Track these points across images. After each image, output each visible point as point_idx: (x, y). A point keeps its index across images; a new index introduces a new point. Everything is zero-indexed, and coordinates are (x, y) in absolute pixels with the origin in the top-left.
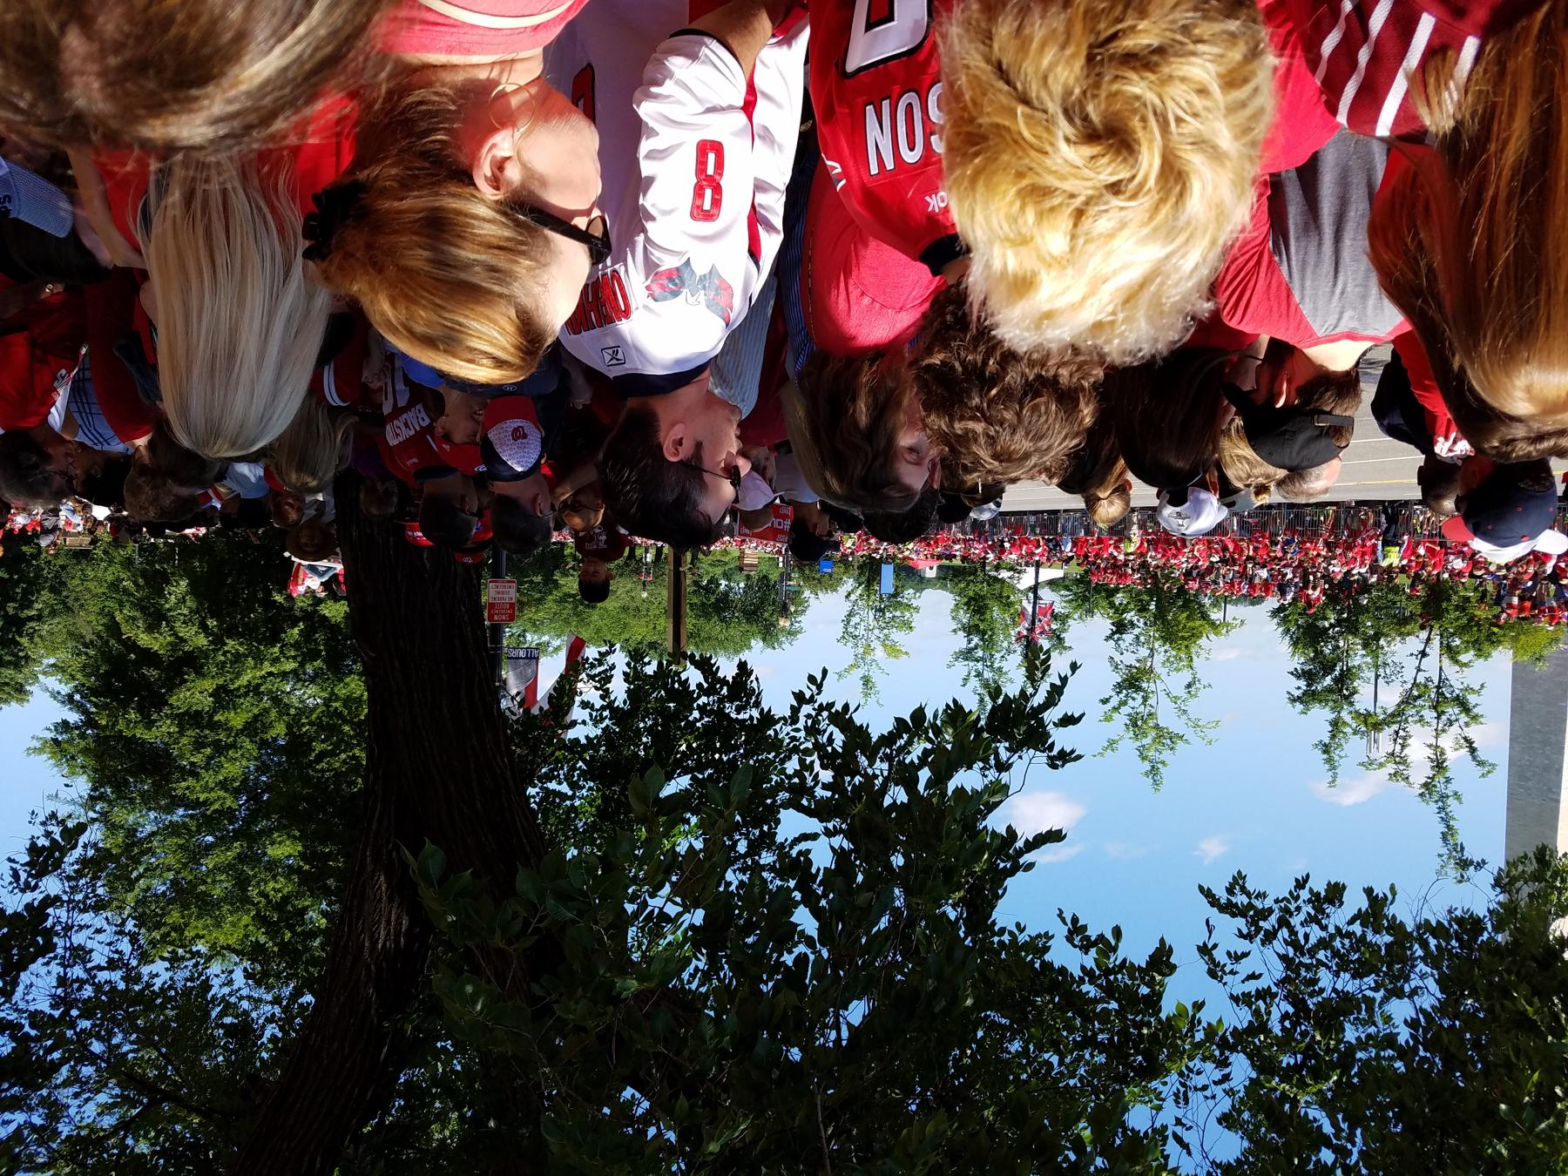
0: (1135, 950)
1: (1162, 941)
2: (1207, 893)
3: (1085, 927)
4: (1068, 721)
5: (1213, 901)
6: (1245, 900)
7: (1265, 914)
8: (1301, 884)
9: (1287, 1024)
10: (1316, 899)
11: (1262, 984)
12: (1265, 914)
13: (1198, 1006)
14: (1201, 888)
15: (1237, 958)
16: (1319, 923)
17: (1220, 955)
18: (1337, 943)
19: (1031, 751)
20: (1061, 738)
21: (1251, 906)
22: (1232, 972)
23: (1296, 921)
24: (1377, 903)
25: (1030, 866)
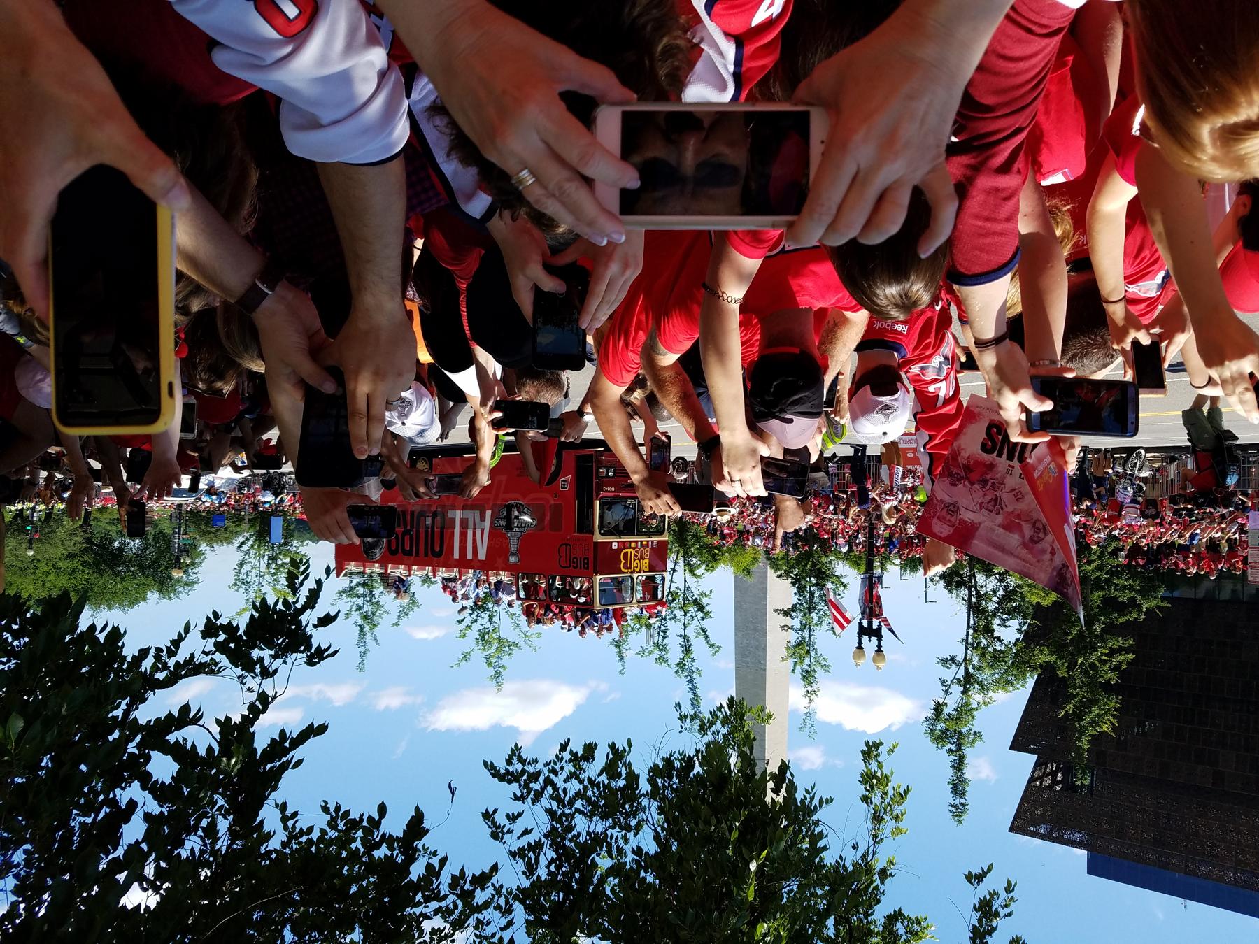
0: (394, 825)
1: (417, 809)
2: (489, 766)
3: (347, 813)
4: (326, 620)
5: (495, 773)
6: (519, 767)
7: (534, 777)
8: (563, 748)
9: (552, 868)
10: (575, 759)
11: (531, 838)
12: (534, 777)
13: (443, 861)
14: (485, 763)
15: (513, 818)
16: (577, 778)
17: (500, 819)
18: (589, 793)
19: (294, 655)
20: (320, 638)
21: (524, 771)
22: (509, 831)
23: (559, 781)
24: (617, 755)
25: (299, 762)
